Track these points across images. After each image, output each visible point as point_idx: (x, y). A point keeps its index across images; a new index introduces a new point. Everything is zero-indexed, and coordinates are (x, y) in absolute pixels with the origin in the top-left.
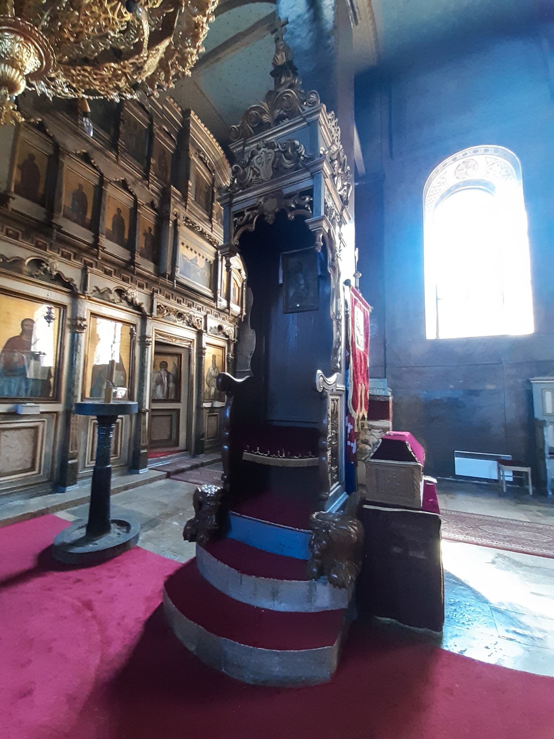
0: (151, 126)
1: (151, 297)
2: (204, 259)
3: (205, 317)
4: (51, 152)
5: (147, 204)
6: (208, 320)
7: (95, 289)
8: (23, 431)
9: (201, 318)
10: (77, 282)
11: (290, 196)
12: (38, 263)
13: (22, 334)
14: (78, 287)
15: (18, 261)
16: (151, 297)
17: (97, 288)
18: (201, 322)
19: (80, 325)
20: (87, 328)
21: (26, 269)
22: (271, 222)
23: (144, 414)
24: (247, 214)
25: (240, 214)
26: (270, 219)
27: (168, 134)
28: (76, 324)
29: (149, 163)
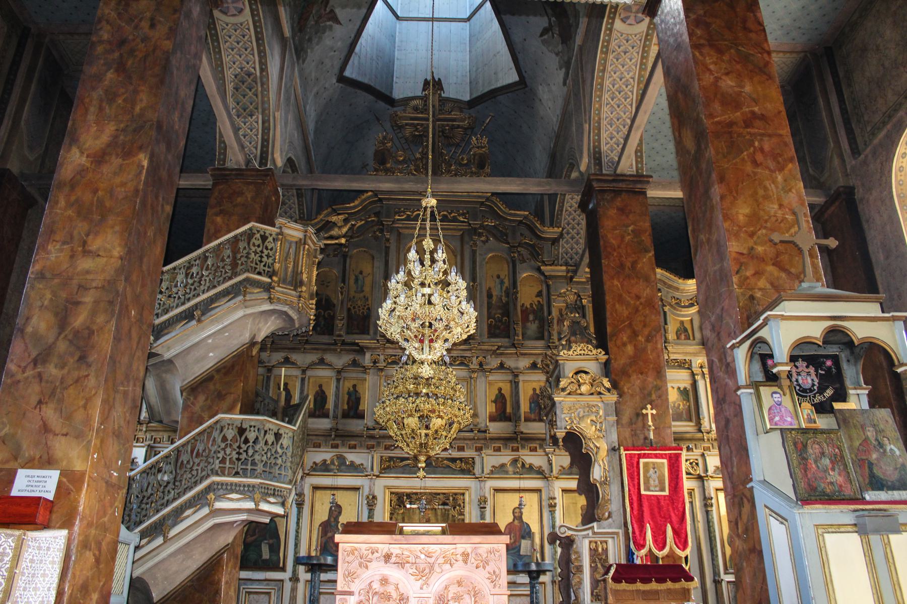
2: (676, 389)
3: (703, 455)
4: (510, 377)
6: (708, 459)
7: (560, 468)
8: (522, 598)
9: (697, 460)
10: (545, 467)
12: (515, 461)
13: (514, 520)
14: (546, 472)
15: (503, 466)
17: (562, 466)
18: (697, 464)
20: (558, 505)
21: (510, 469)
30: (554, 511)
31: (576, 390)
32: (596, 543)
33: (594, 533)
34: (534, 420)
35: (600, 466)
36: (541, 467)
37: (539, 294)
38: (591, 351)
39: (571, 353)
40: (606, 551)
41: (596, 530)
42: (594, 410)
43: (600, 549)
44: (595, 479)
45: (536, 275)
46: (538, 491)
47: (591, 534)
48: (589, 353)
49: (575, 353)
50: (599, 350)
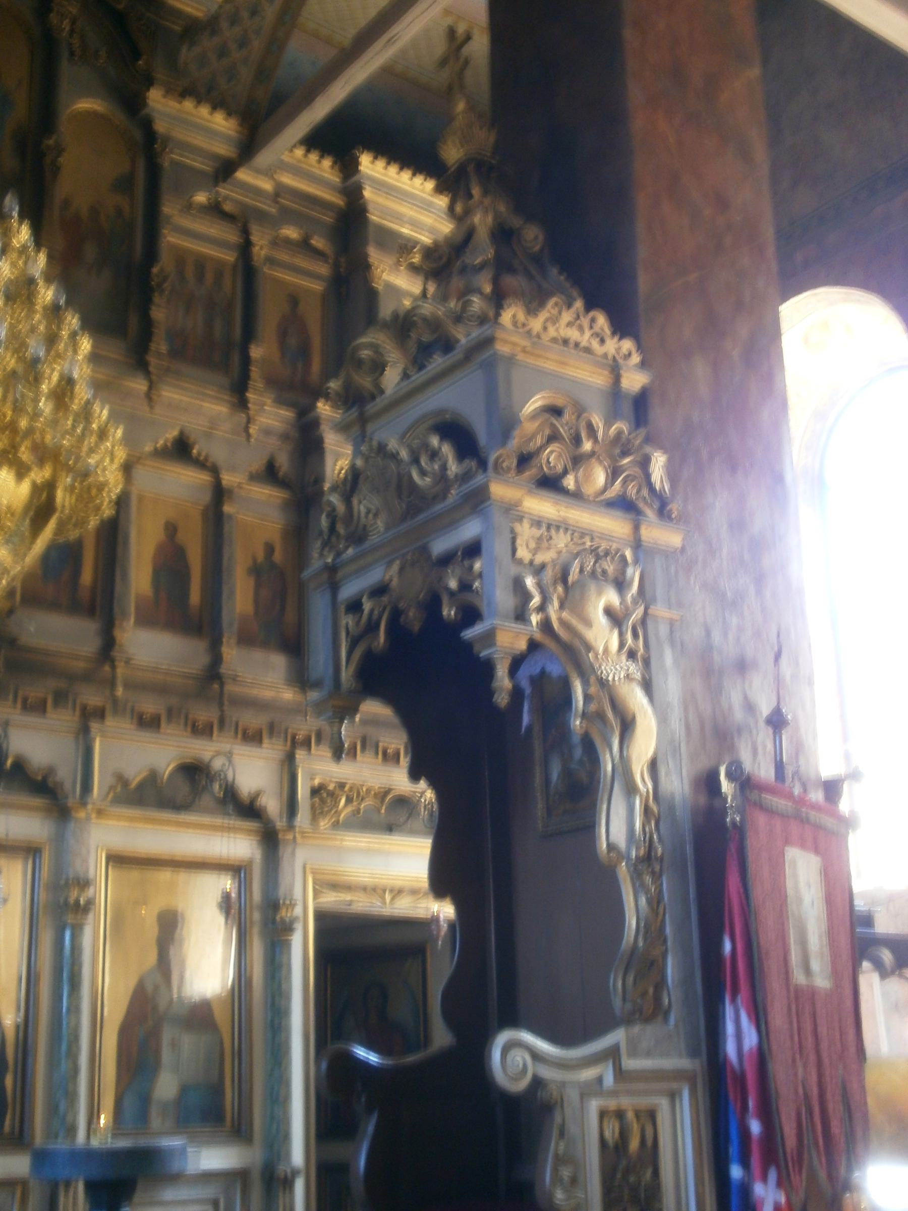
0: (246, 248)
1: (289, 763)
5: (254, 478)
11: (446, 560)
16: (289, 763)
19: (77, 902)
22: (416, 627)
23: (288, 1183)
24: (367, 606)
25: (355, 606)
26: (413, 618)
27: (304, 245)
28: (66, 903)
29: (246, 360)
30: (77, 930)
31: (565, 472)
32: (620, 1115)
33: (620, 1074)
34: (54, 606)
35: (631, 789)
36: (50, 771)
37: (124, 184)
38: (602, 341)
39: (536, 324)
40: (650, 1152)
41: (630, 1064)
42: (610, 567)
43: (634, 1144)
44: (611, 847)
45: (120, 118)
46: (31, 851)
47: (609, 1080)
48: (595, 344)
49: (552, 332)
50: (627, 345)
